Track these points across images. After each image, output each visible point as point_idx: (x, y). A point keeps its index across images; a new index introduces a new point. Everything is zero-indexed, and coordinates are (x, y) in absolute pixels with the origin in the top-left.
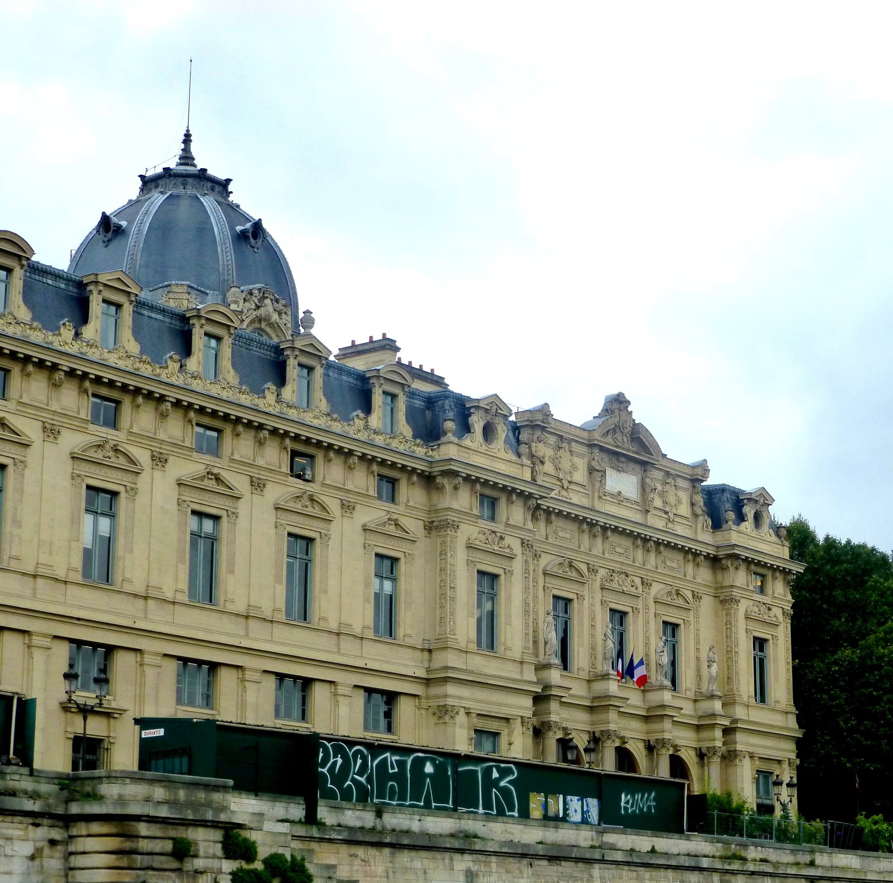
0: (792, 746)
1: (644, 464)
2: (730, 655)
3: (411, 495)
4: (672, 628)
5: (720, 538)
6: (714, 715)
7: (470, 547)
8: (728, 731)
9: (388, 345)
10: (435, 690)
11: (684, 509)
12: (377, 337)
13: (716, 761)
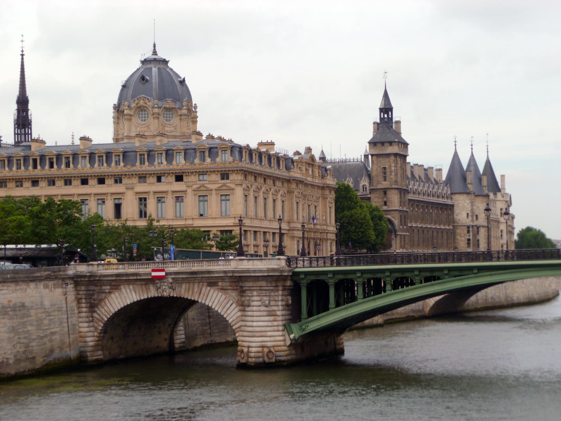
0: (335, 235)
1: (313, 165)
2: (326, 212)
3: (286, 184)
4: (316, 206)
5: (324, 181)
6: (325, 230)
7: (296, 197)
8: (327, 233)
9: (272, 144)
10: (290, 232)
11: (317, 175)
12: (269, 141)
13: (325, 241)
